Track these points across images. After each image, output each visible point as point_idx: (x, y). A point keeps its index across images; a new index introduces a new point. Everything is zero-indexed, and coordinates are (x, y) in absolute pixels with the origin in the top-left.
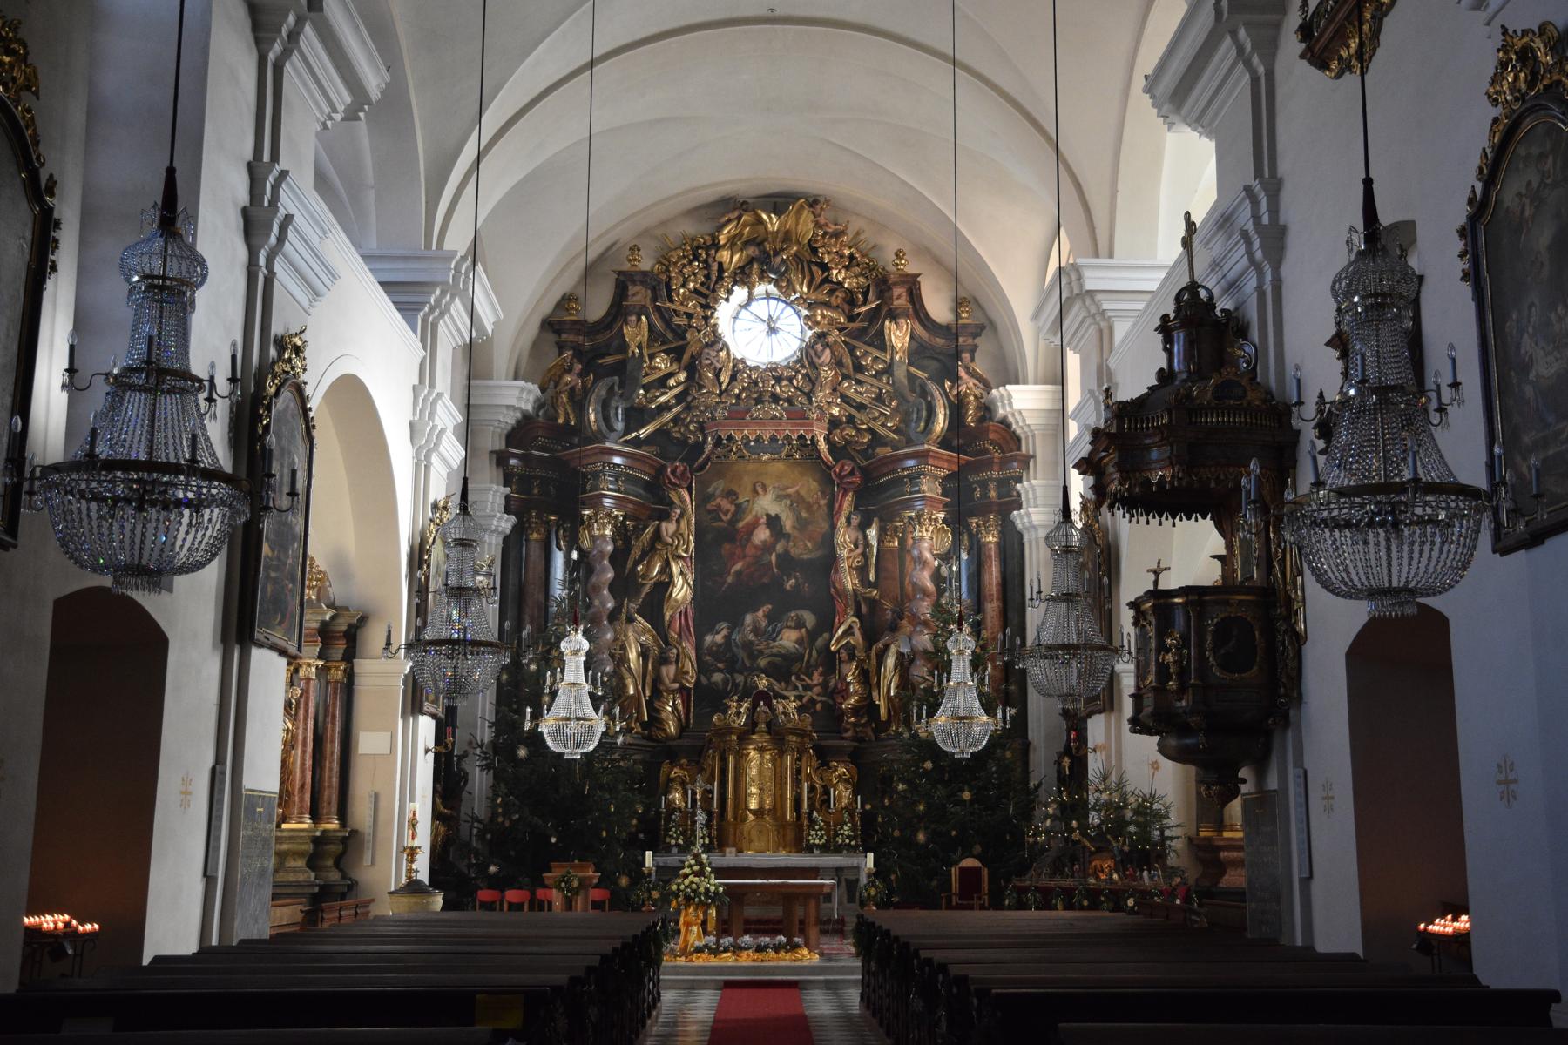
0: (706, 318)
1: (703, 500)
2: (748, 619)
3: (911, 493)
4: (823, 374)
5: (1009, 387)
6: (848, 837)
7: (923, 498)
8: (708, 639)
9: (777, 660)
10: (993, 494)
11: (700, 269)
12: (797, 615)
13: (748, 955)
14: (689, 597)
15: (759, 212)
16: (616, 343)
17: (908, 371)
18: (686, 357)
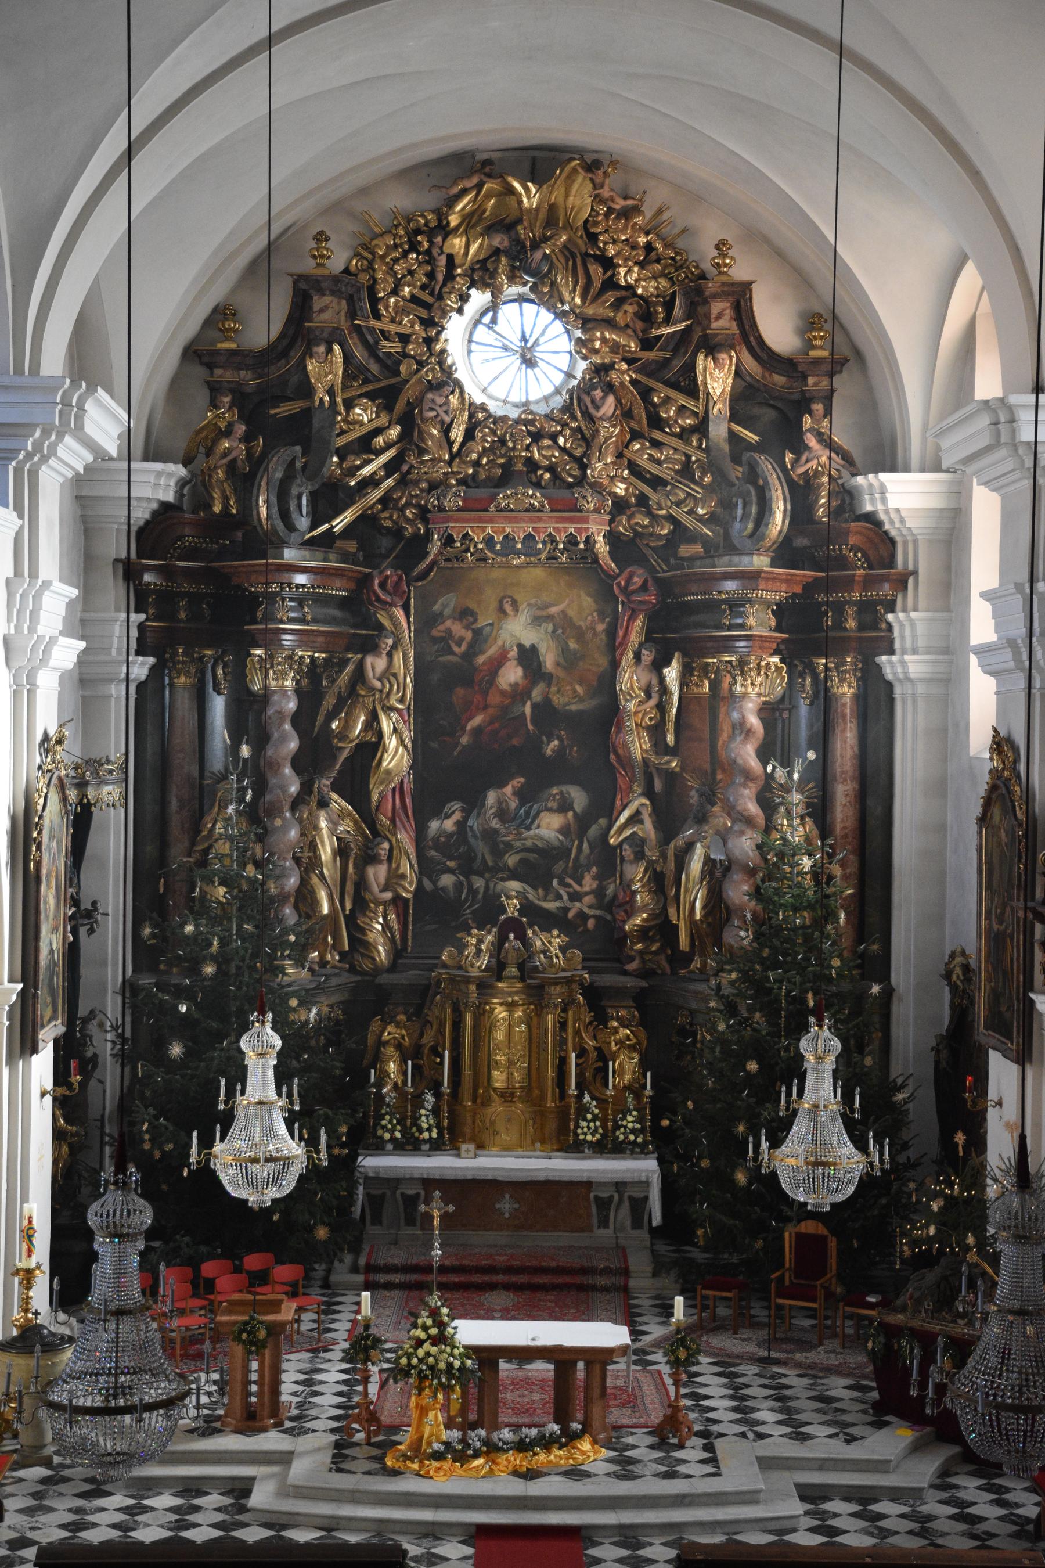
0: (429, 342)
1: (426, 623)
2: (491, 797)
3: (731, 627)
4: (603, 433)
5: (883, 476)
6: (633, 1131)
7: (748, 638)
8: (434, 825)
9: (532, 857)
10: (851, 624)
11: (420, 264)
12: (561, 793)
13: (507, 1460)
15: (510, 179)
16: (295, 379)
17: (731, 433)
18: (400, 406)
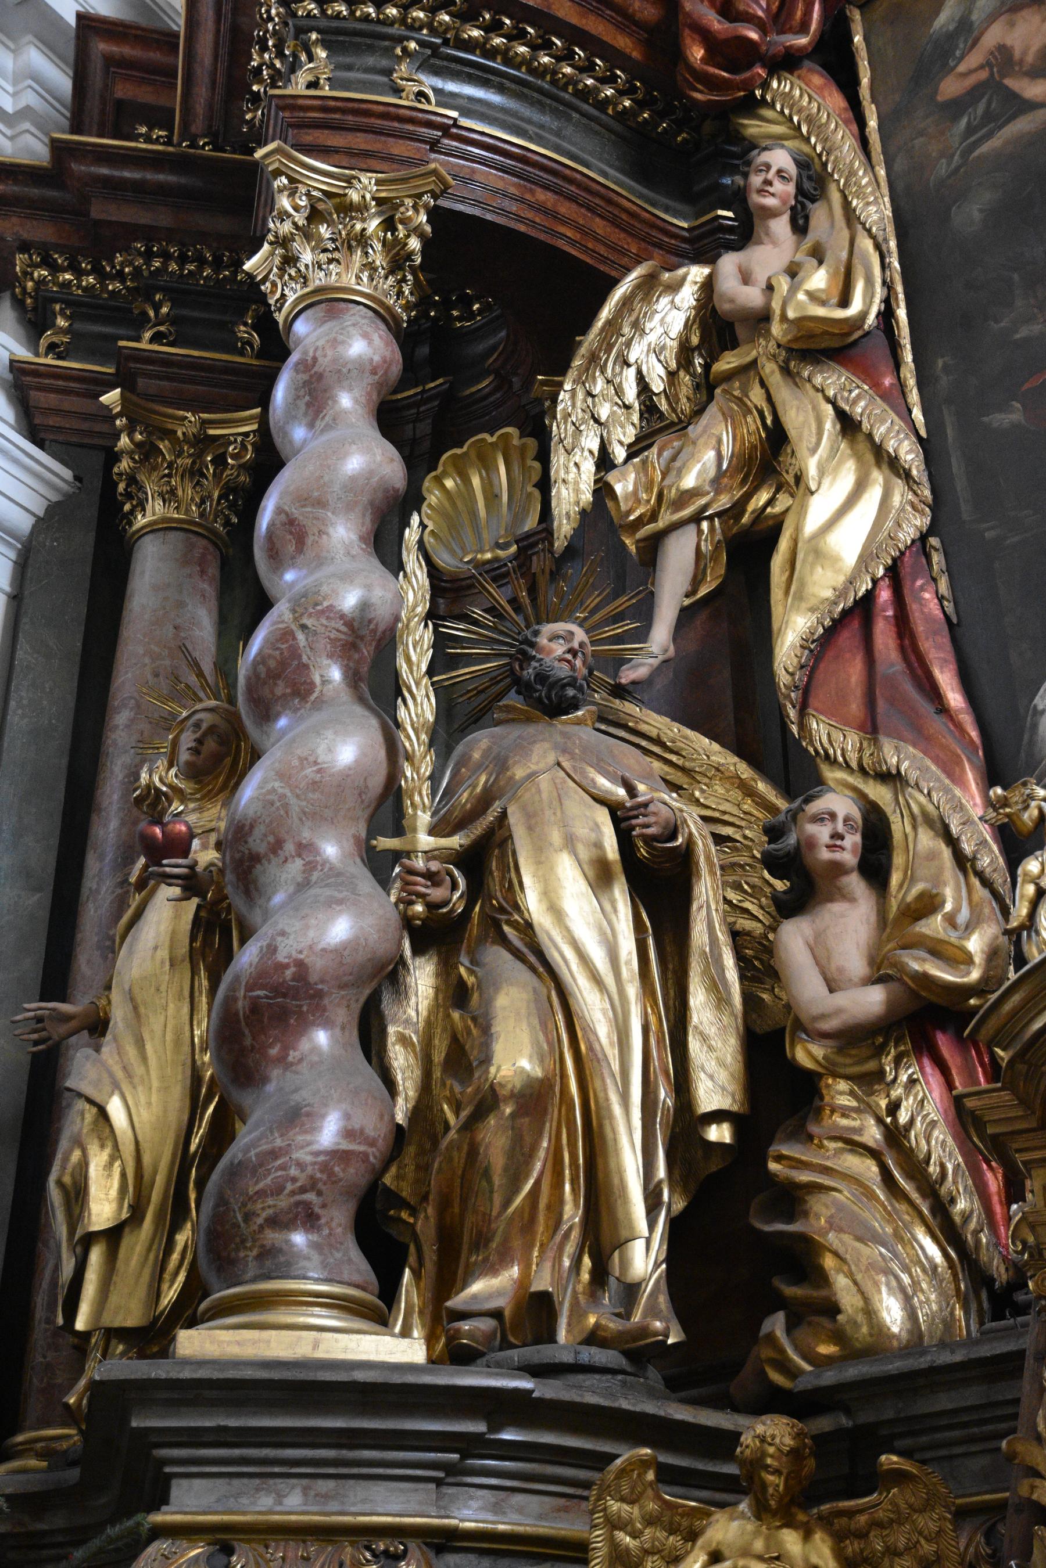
14: (917, 522)
